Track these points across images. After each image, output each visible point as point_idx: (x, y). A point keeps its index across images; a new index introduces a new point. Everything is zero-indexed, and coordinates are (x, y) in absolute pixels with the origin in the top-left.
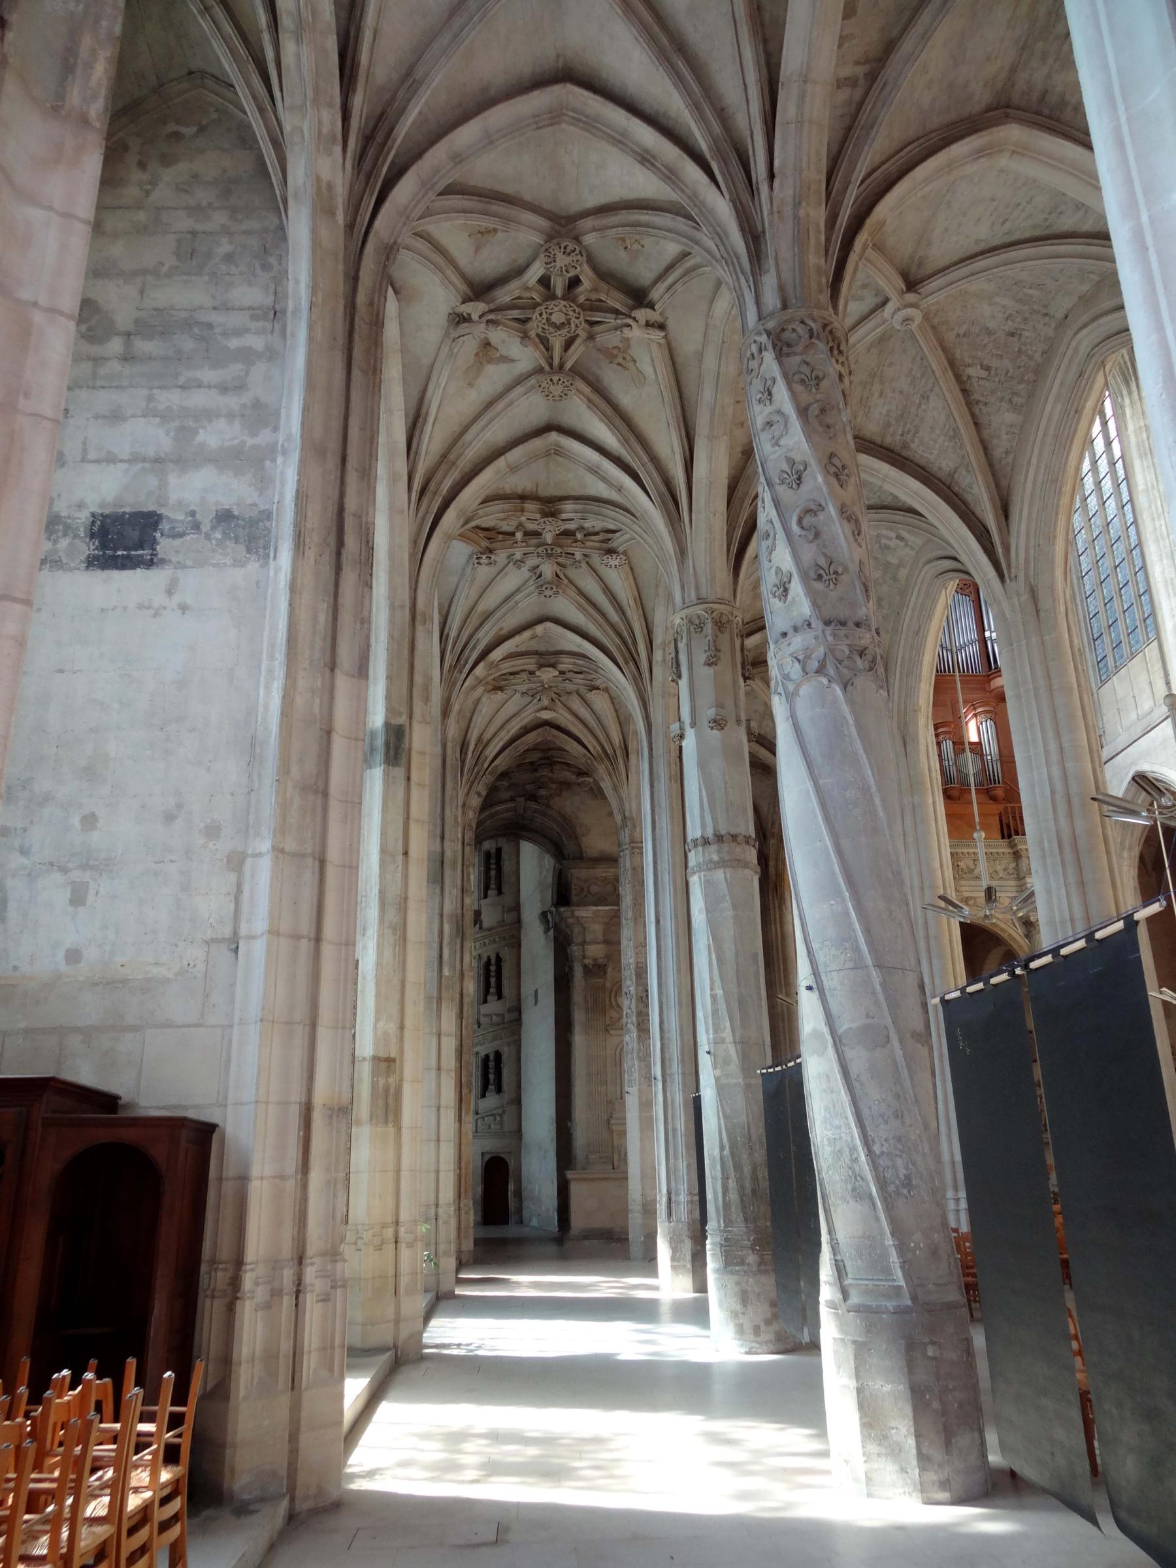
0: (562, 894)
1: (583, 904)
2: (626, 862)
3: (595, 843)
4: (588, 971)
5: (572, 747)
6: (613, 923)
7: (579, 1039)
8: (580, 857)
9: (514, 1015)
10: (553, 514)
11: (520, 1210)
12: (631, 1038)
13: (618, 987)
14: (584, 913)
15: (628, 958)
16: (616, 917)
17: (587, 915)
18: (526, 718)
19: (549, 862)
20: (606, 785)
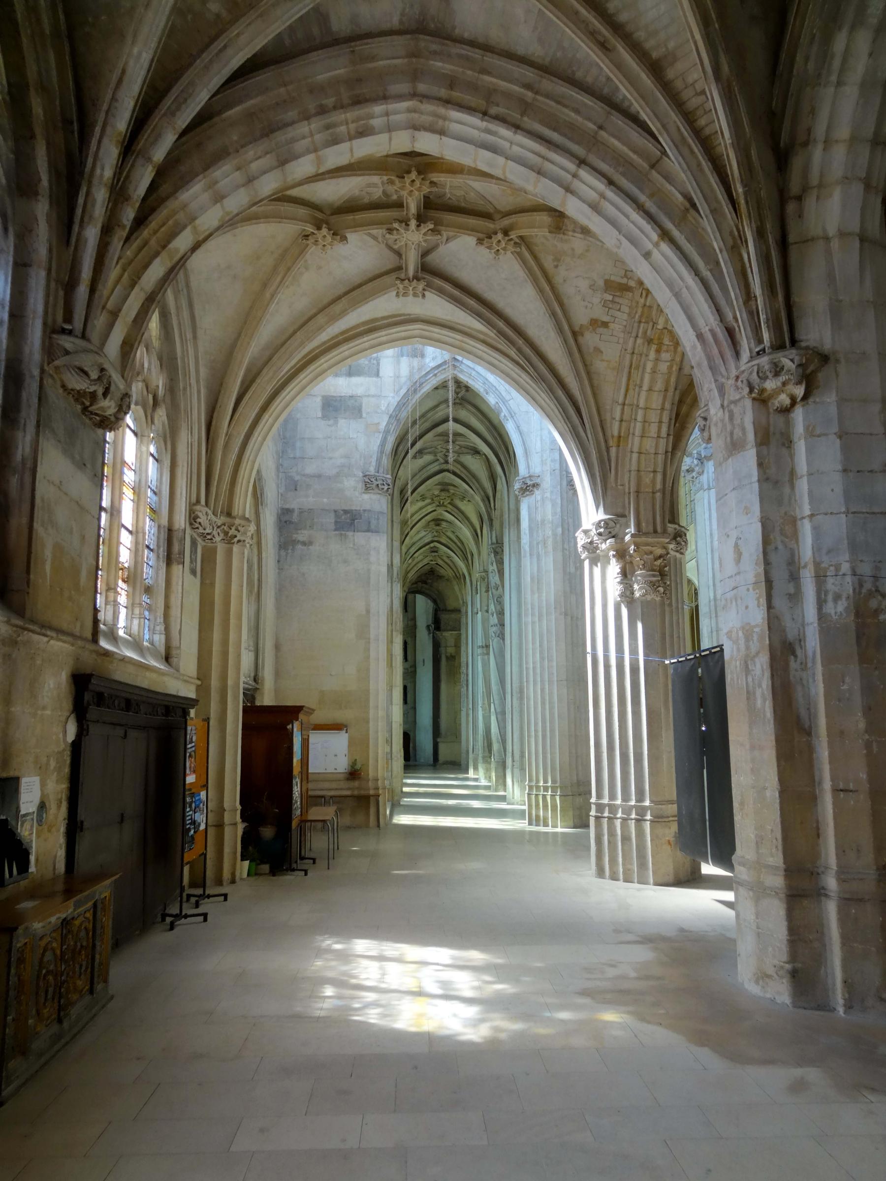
0: (437, 625)
1: (444, 631)
2: (463, 620)
3: (451, 604)
4: (447, 658)
5: (442, 572)
6: (458, 640)
7: (443, 687)
8: (446, 610)
9: (413, 669)
10: (438, 525)
11: (415, 755)
12: (464, 690)
13: (460, 666)
14: (447, 634)
15: (463, 659)
16: (459, 636)
17: (448, 636)
18: (426, 561)
19: (430, 604)
20: (456, 588)
